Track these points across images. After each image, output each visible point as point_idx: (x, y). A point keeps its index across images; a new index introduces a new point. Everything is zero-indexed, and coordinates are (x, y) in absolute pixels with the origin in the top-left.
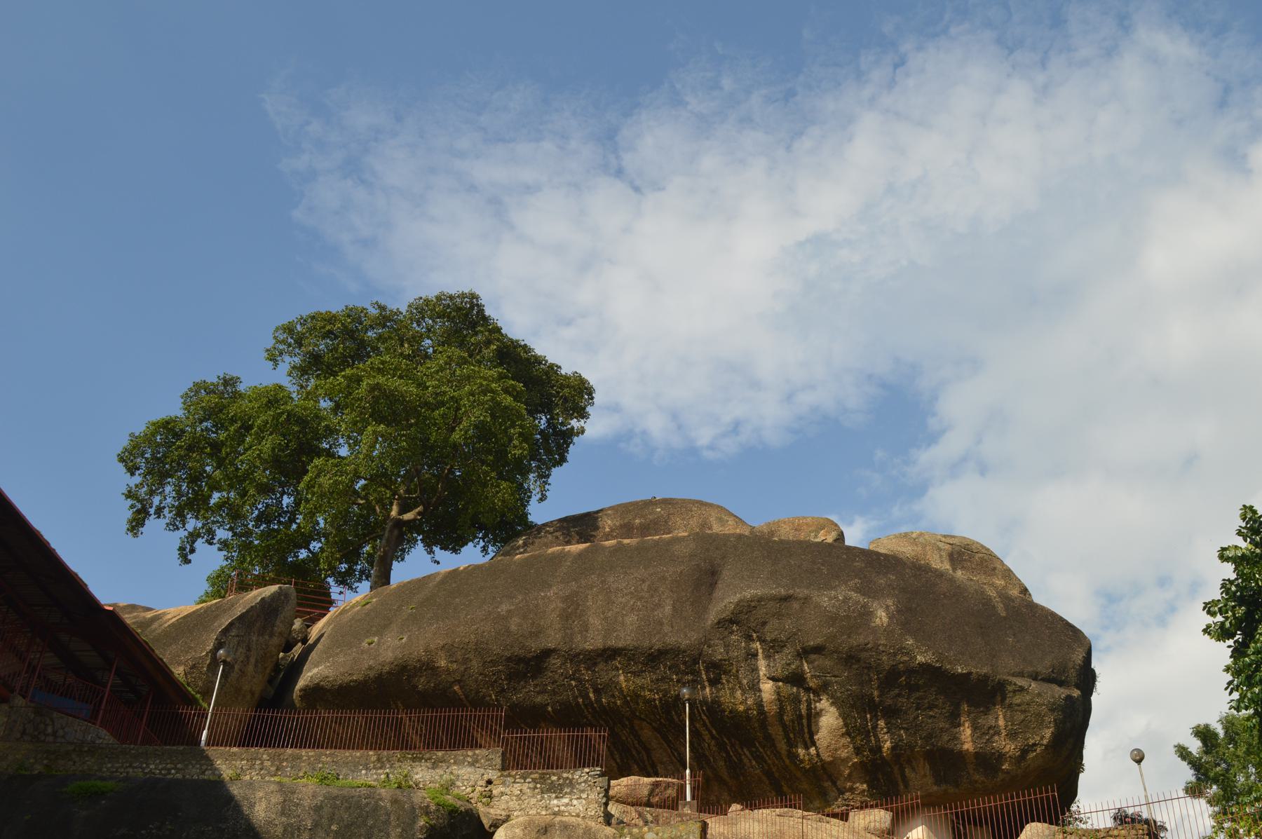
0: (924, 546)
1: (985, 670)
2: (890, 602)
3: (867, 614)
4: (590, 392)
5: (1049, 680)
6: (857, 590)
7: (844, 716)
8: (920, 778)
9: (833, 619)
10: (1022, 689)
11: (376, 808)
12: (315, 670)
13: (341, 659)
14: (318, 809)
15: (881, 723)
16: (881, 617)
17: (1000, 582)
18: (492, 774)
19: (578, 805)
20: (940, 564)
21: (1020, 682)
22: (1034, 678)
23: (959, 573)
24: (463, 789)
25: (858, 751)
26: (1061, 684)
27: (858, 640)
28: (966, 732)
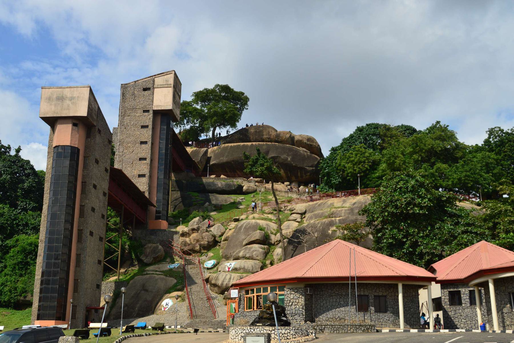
0: (303, 138)
1: (302, 166)
2: (290, 157)
3: (287, 159)
4: (249, 99)
5: (310, 167)
6: (286, 155)
7: (284, 170)
8: (293, 178)
9: (283, 159)
10: (306, 169)
11: (231, 185)
12: (214, 162)
13: (217, 161)
14: (225, 185)
15: (289, 172)
16: (289, 159)
17: (315, 144)
18: (242, 180)
19: (252, 184)
20: (305, 141)
21: (306, 168)
22: (308, 167)
23: (308, 143)
24: (239, 182)
25: (286, 175)
26: (312, 167)
27: (286, 162)
28: (299, 174)
